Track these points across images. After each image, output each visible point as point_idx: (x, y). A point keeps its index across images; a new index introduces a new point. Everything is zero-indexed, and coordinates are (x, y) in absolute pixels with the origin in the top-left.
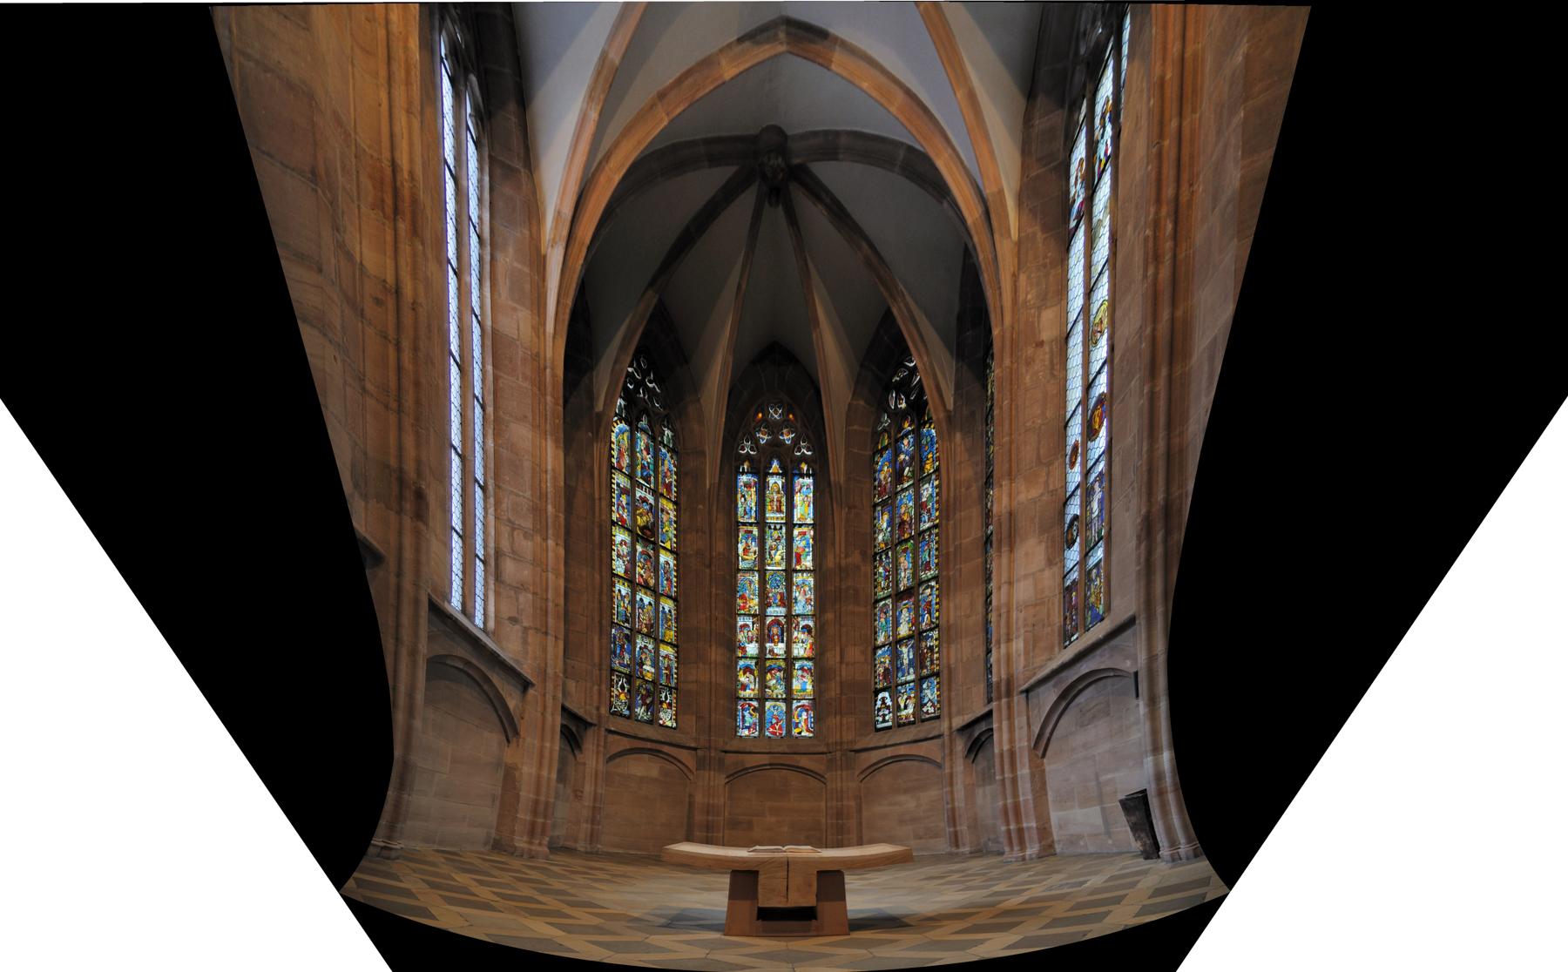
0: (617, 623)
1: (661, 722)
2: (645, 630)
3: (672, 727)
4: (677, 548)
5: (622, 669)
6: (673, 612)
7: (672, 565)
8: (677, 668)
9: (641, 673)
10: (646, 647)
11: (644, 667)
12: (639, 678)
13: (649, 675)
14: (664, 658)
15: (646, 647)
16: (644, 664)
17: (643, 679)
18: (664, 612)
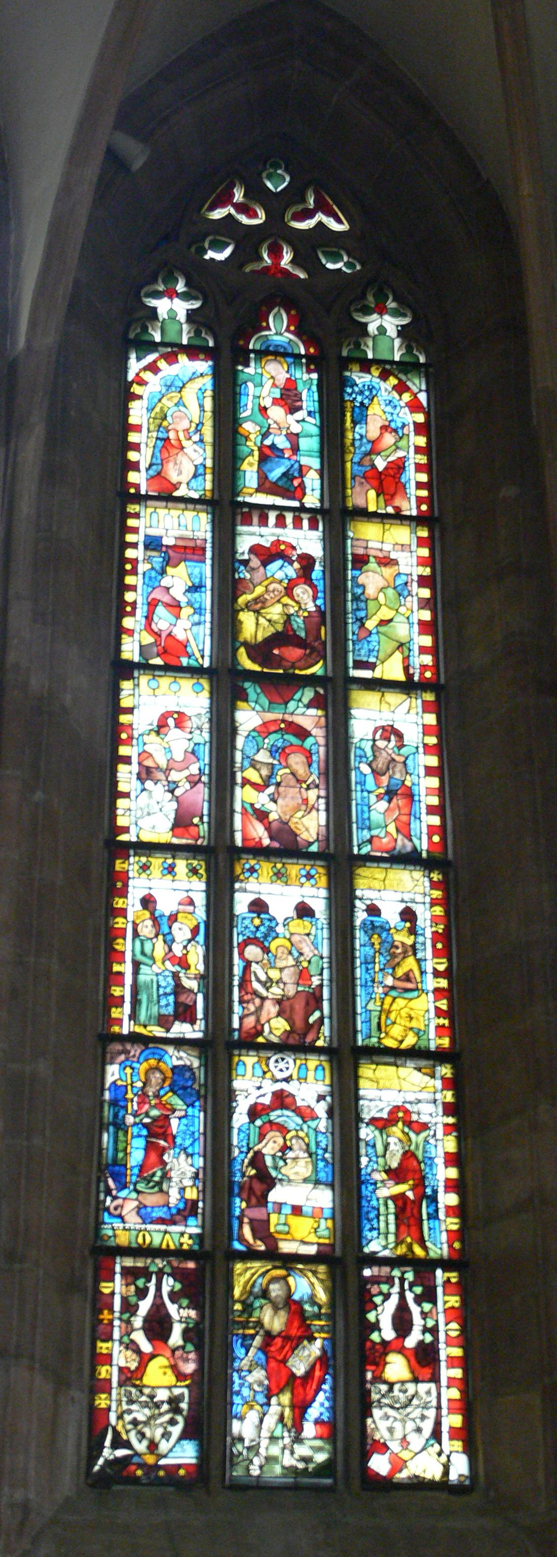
0: (134, 1038)
1: (379, 1464)
2: (275, 1029)
3: (443, 1486)
4: (436, 667)
5: (156, 1236)
6: (424, 915)
7: (413, 735)
8: (451, 1160)
9: (261, 1229)
10: (282, 1100)
11: (274, 1196)
12: (250, 1255)
13: (302, 1227)
14: (382, 1124)
15: (282, 1100)
16: (269, 1182)
17: (272, 1255)
18: (372, 929)
